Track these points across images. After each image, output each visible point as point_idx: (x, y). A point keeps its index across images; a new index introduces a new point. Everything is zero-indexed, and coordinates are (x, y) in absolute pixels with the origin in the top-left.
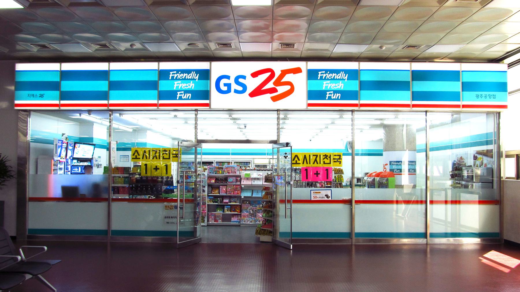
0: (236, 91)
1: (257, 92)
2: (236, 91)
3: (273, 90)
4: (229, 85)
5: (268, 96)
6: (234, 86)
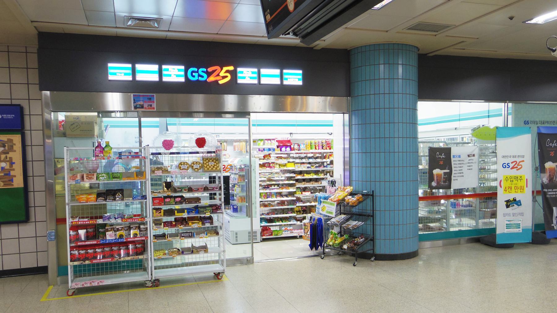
0: (507, 167)
1: (513, 168)
2: (507, 167)
3: (517, 167)
4: (506, 166)
5: (516, 169)
6: (507, 166)
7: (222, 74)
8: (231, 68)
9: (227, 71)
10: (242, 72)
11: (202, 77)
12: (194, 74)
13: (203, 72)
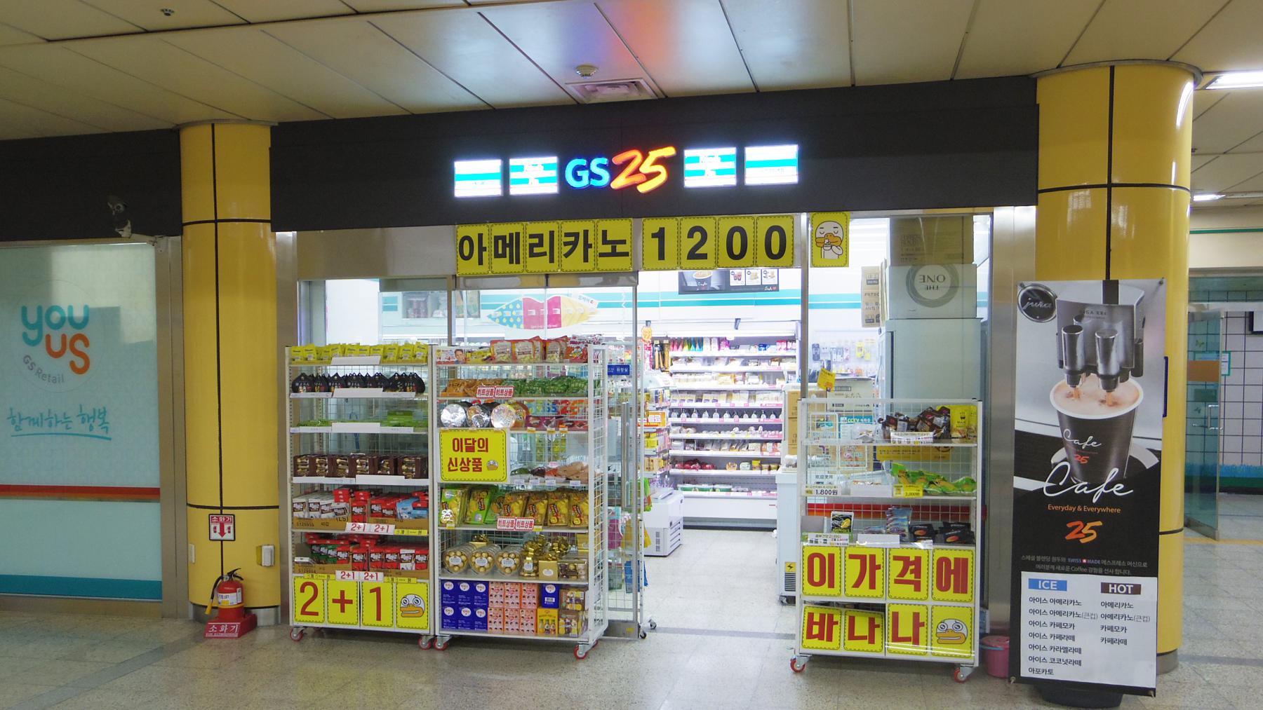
7: (647, 168)
8: (669, 151)
9: (659, 161)
10: (696, 160)
11: (599, 178)
12: (579, 173)
13: (600, 166)
